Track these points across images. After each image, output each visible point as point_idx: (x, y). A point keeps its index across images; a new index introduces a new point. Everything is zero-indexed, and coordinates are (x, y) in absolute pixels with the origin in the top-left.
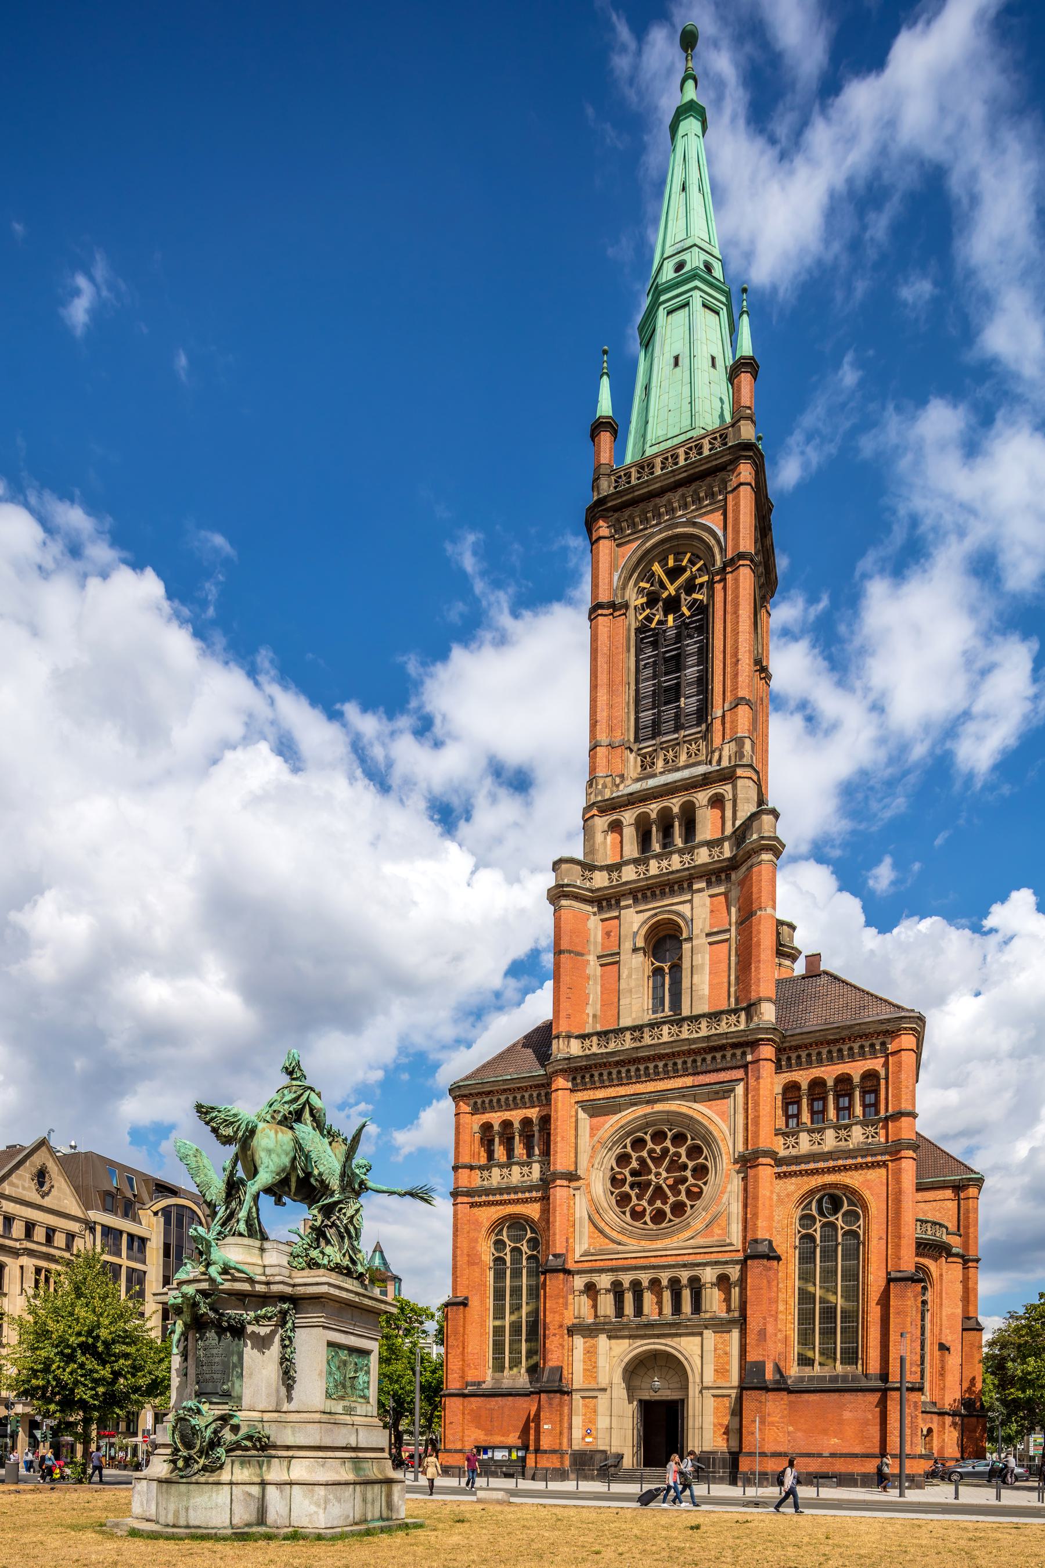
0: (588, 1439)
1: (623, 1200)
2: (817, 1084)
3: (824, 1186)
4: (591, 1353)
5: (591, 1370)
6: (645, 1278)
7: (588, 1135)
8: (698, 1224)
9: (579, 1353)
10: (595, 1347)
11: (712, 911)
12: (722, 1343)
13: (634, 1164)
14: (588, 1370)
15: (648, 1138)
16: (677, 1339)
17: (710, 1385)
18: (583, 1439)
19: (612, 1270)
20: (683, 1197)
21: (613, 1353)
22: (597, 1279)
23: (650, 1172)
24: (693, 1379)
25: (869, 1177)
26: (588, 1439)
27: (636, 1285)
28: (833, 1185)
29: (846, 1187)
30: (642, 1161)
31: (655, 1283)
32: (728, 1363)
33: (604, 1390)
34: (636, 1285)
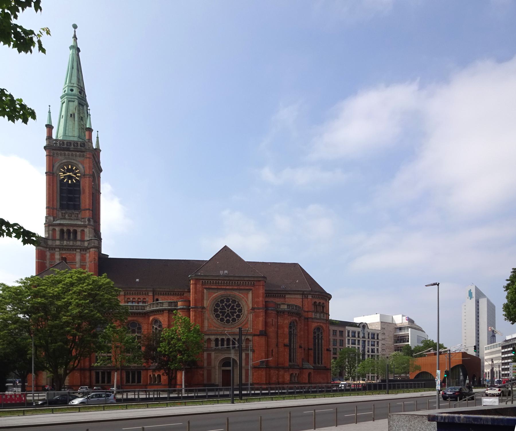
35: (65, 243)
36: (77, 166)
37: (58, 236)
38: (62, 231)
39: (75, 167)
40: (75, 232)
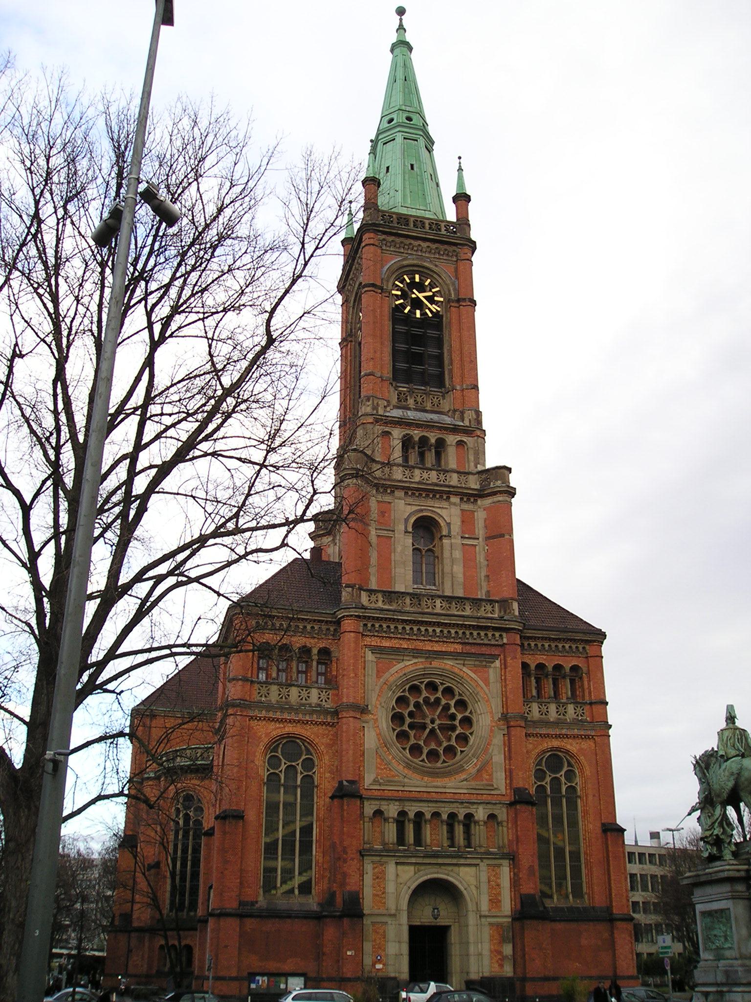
0: (379, 966)
1: (402, 736)
2: (541, 667)
3: (552, 749)
4: (380, 877)
5: (380, 895)
6: (427, 810)
7: (375, 675)
8: (471, 768)
9: (368, 879)
10: (383, 872)
11: (463, 522)
12: (494, 876)
13: (411, 708)
14: (378, 895)
15: (441, 688)
16: (456, 869)
17: (487, 913)
18: (374, 965)
19: (400, 800)
20: (453, 742)
21: (400, 880)
22: (386, 807)
23: (424, 716)
24: (471, 906)
25: (583, 747)
26: (379, 966)
27: (420, 815)
28: (558, 749)
29: (567, 752)
30: (417, 705)
31: (436, 815)
32: (499, 894)
33: (394, 915)
34: (420, 815)
35: (417, 475)
36: (435, 276)
37: (397, 454)
38: (407, 443)
39: (429, 281)
40: (441, 444)
